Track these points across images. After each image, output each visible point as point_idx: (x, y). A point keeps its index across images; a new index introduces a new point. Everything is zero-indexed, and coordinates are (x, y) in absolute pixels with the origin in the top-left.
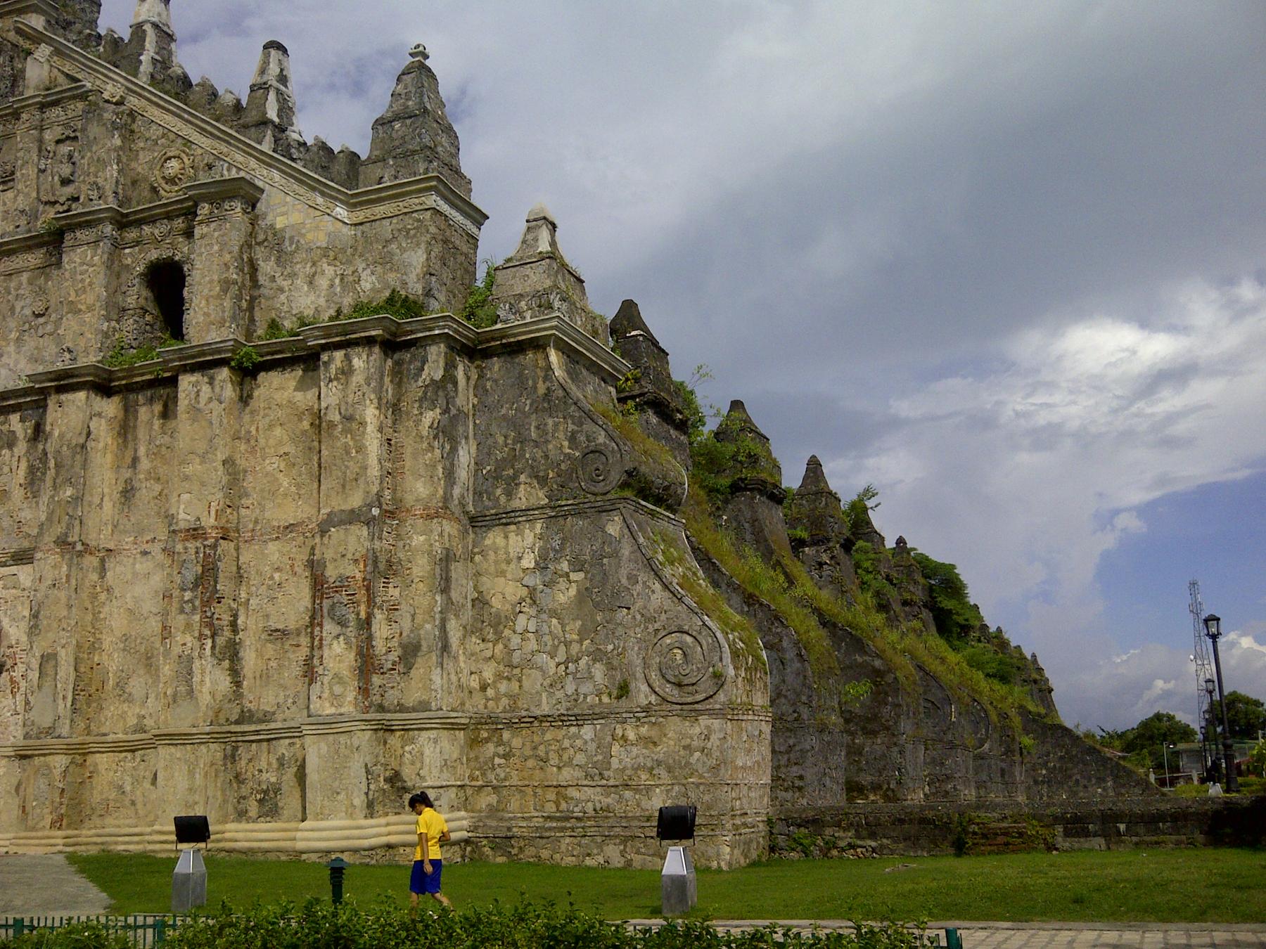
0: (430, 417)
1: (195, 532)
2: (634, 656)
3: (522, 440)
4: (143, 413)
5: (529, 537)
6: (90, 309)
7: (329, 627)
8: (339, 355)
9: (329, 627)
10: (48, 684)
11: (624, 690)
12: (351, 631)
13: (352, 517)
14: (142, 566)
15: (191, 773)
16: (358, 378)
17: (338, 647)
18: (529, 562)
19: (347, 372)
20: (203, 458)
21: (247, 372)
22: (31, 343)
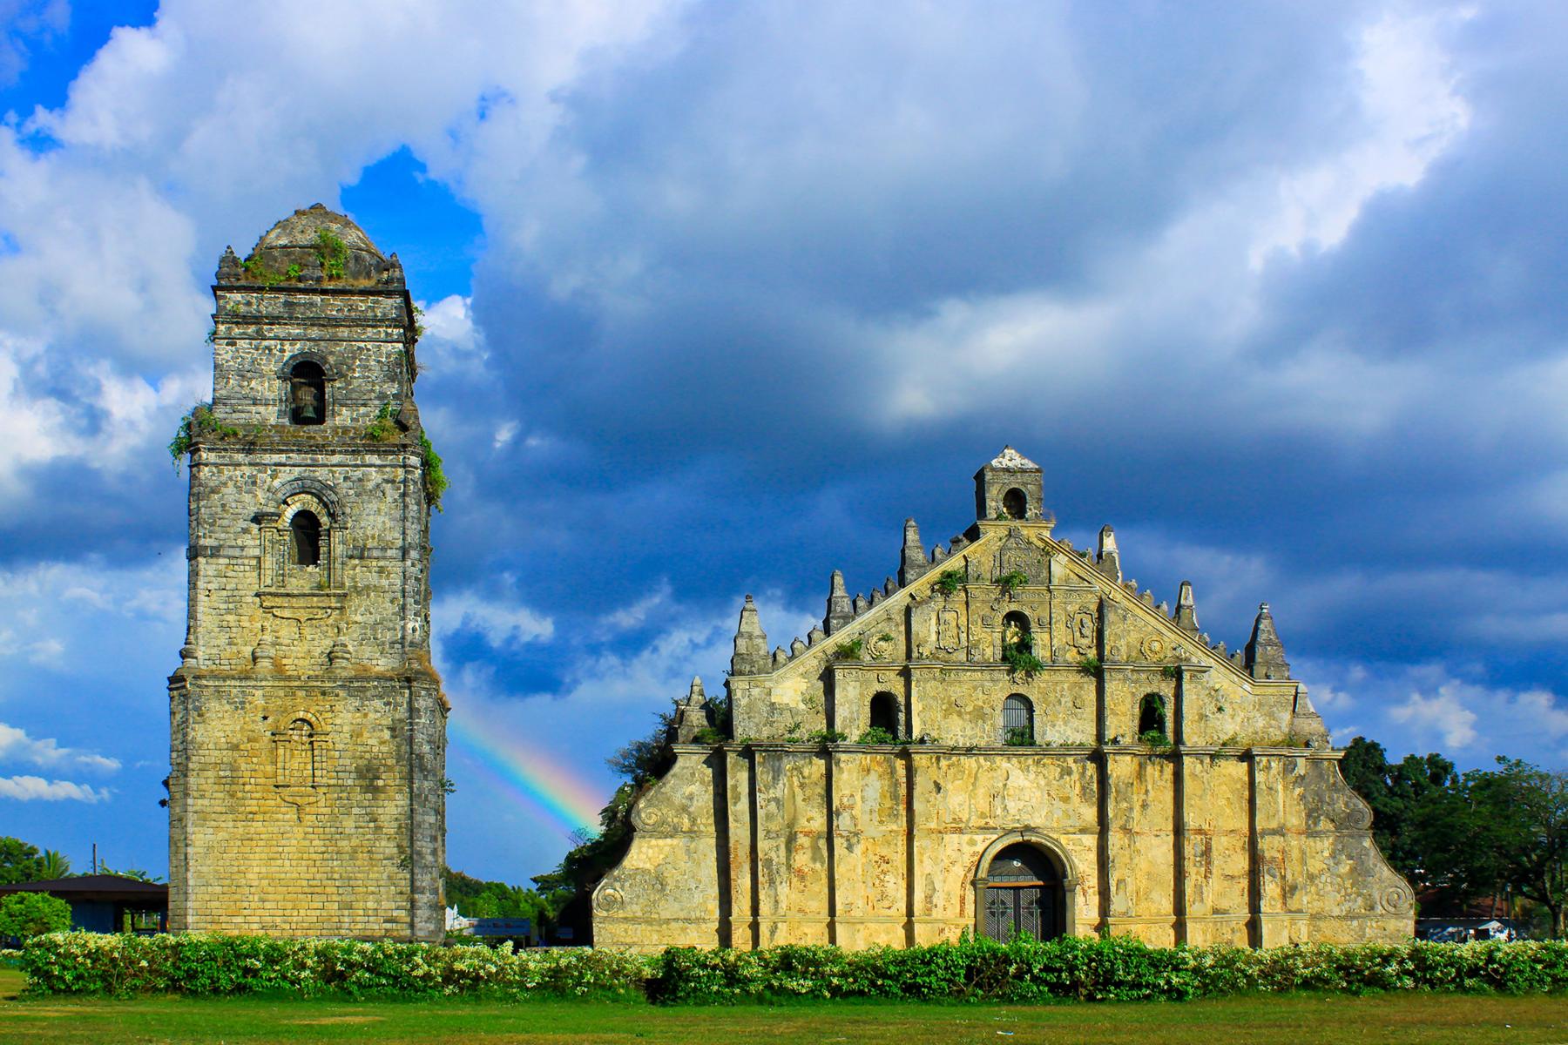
0: (1298, 791)
1: (1200, 831)
2: (1377, 896)
3: (1321, 801)
4: (1149, 768)
5: (1326, 844)
6: (1124, 714)
7: (1267, 877)
8: (1264, 759)
9: (1267, 877)
10: (1121, 892)
11: (1372, 908)
12: (1278, 879)
13: (1274, 832)
14: (1155, 841)
15: (1205, 933)
16: (1273, 772)
17: (1273, 886)
18: (1326, 854)
19: (1268, 768)
20: (1200, 797)
21: (1213, 757)
22: (1075, 723)
